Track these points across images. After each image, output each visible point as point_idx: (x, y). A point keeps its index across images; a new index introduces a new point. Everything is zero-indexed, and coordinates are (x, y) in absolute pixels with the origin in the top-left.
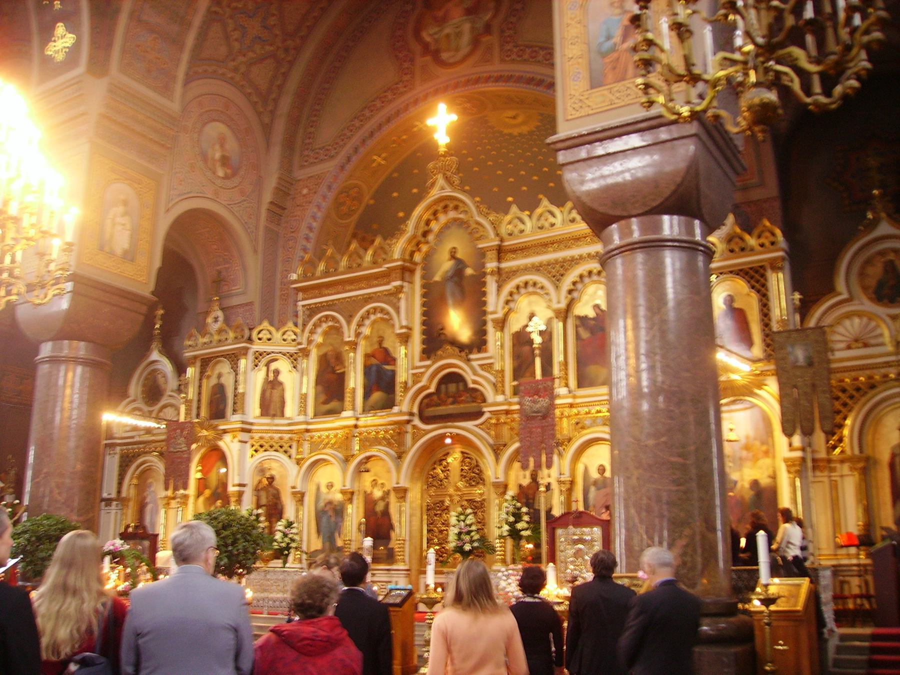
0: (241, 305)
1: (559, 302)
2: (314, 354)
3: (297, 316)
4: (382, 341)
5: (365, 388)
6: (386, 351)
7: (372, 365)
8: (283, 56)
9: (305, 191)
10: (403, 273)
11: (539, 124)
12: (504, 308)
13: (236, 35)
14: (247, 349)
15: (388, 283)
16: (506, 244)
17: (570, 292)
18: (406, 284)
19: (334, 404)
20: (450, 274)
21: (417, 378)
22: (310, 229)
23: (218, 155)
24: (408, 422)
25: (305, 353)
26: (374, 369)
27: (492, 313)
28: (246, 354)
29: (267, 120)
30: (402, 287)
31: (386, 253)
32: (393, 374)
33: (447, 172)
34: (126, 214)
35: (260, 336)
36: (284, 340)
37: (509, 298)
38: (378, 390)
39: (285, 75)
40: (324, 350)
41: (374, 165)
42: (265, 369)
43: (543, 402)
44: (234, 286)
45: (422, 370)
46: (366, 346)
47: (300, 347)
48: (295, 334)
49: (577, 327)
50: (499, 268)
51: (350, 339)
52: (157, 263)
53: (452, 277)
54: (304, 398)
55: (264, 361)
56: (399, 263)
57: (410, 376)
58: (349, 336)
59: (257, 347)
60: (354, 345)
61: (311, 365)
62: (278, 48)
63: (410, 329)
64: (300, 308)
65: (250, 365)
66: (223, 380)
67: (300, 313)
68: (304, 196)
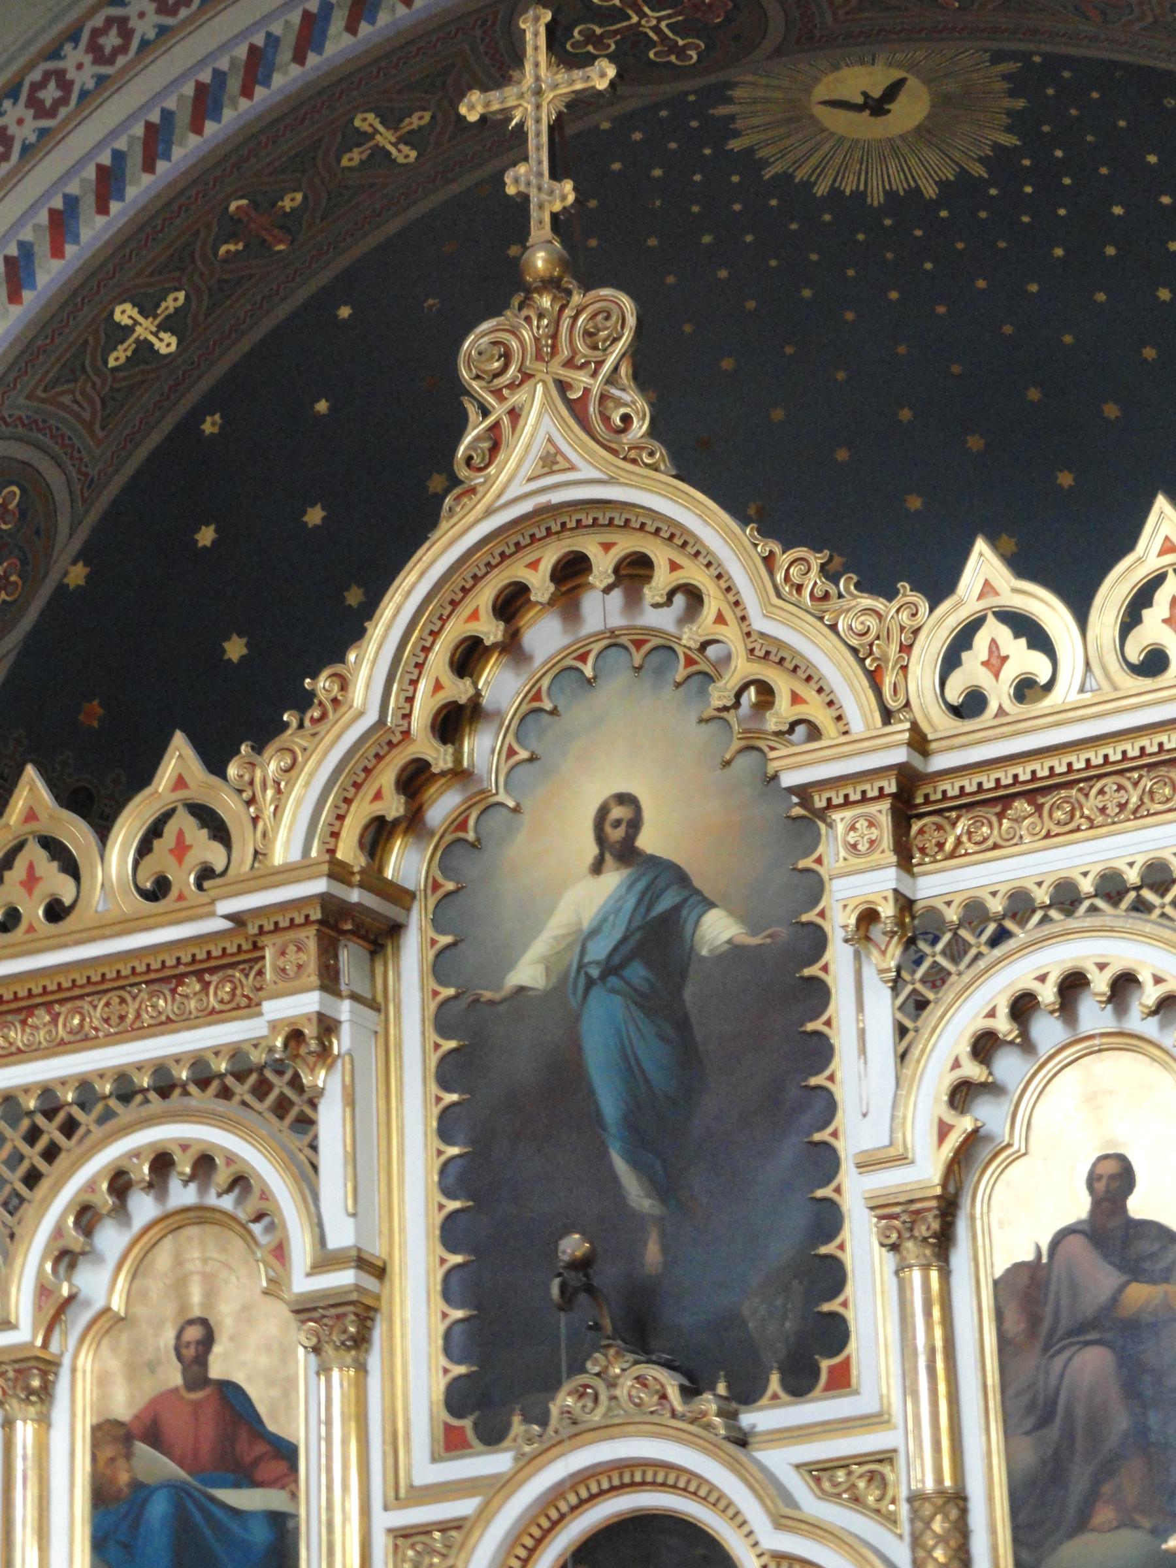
4: (208, 1340)
7: (141, 1492)
10: (328, 951)
11: (1009, 140)
12: (944, 1130)
15: (250, 1006)
16: (939, 763)
18: (344, 1010)
20: (599, 950)
27: (868, 1163)
30: (327, 1026)
31: (219, 831)
33: (582, 379)
37: (973, 1071)
41: (118, 357)
45: (464, 1507)
46: (102, 1381)
50: (905, 904)
53: (612, 968)
56: (319, 886)
57: (381, 1543)
63: (380, 1272)
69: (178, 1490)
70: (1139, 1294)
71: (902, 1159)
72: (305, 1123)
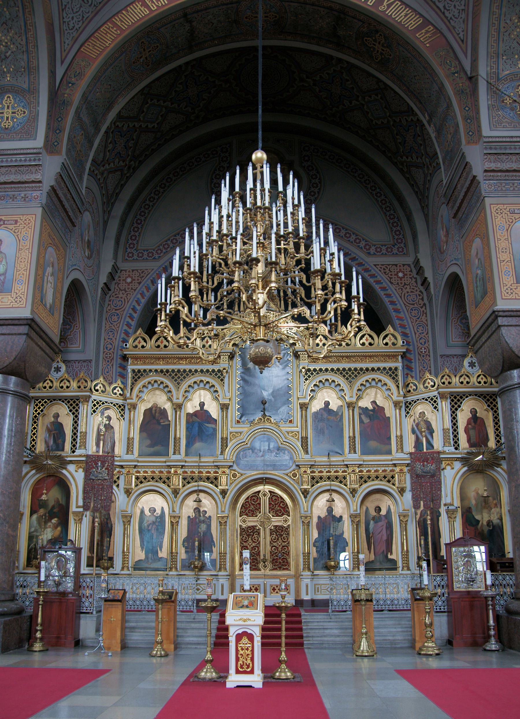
0: (79, 361)
1: (352, 397)
2: (142, 408)
3: (123, 376)
5: (188, 438)
6: (207, 412)
8: (126, 172)
9: (129, 280)
13: (110, 147)
14: (90, 397)
17: (359, 390)
19: (157, 448)
21: (235, 434)
22: (134, 310)
23: (87, 239)
24: (231, 466)
25: (134, 407)
26: (196, 425)
28: (88, 402)
29: (106, 219)
32: (215, 430)
34: (52, 274)
35: (96, 388)
36: (116, 394)
38: (199, 442)
39: (122, 186)
40: (149, 406)
42: (100, 415)
43: (431, 467)
44: (72, 344)
47: (129, 401)
48: (122, 390)
49: (360, 414)
51: (177, 401)
52: (61, 321)
54: (130, 442)
55: (100, 409)
58: (178, 396)
59: (95, 396)
60: (178, 407)
61: (139, 417)
62: (126, 165)
64: (129, 370)
65: (90, 411)
66: (60, 420)
67: (130, 375)
68: (129, 284)
69: (199, 423)
70: (329, 417)
71: (305, 397)
72: (222, 380)
